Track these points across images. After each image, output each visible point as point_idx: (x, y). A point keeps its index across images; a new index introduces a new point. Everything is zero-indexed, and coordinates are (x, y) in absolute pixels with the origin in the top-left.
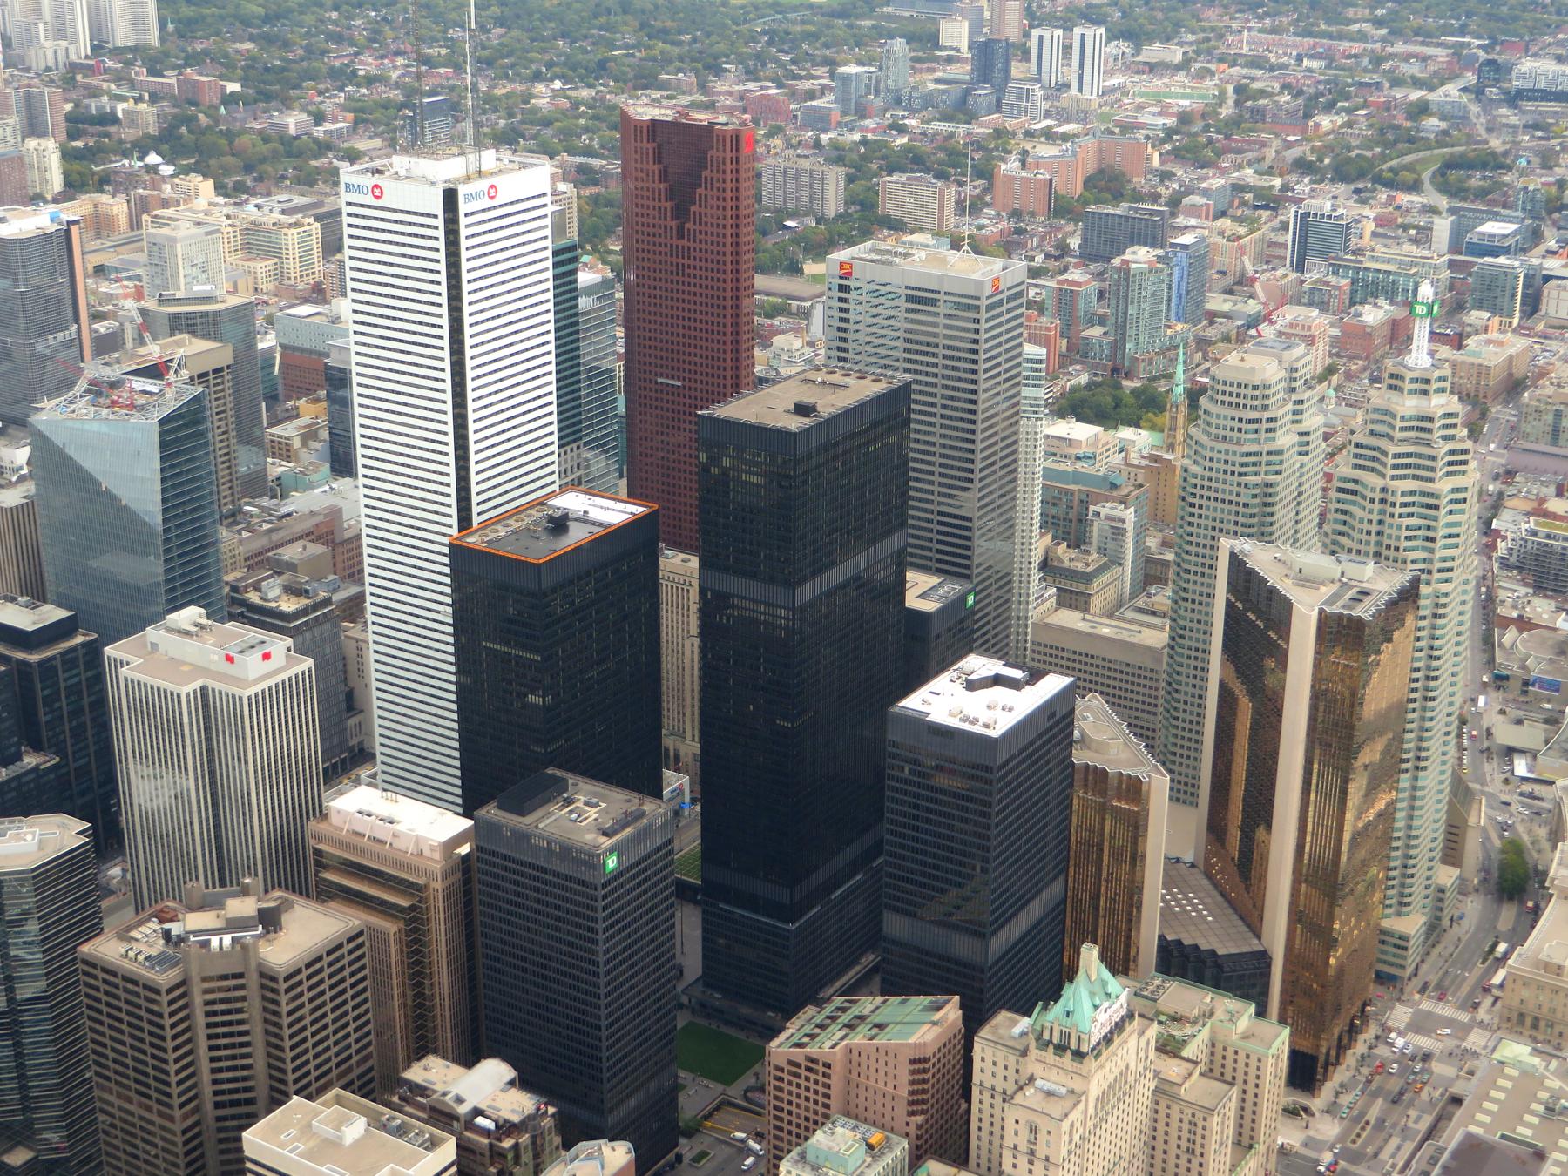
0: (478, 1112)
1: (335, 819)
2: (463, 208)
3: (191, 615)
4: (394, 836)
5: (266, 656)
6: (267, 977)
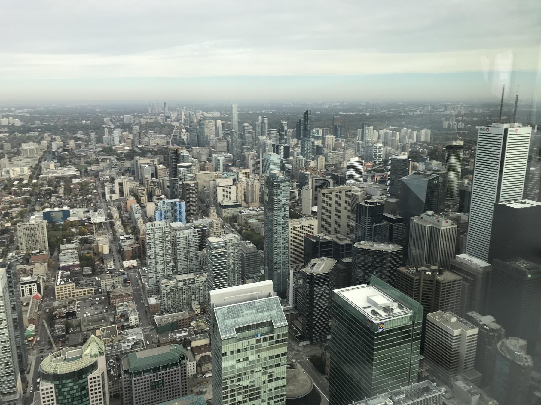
0: (486, 325)
1: (457, 259)
2: (509, 133)
3: (430, 213)
4: (471, 264)
5: (447, 222)
6: (438, 282)
